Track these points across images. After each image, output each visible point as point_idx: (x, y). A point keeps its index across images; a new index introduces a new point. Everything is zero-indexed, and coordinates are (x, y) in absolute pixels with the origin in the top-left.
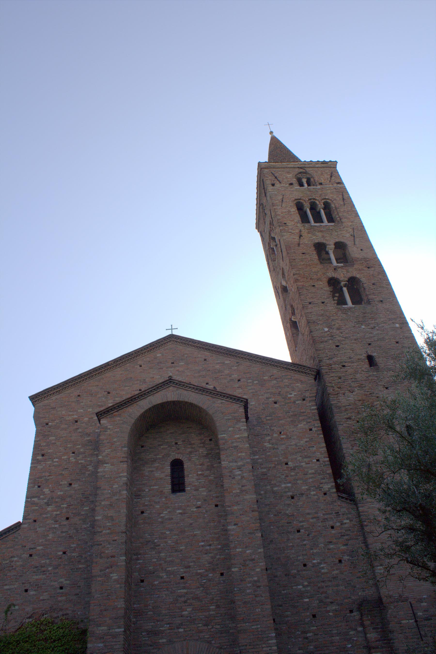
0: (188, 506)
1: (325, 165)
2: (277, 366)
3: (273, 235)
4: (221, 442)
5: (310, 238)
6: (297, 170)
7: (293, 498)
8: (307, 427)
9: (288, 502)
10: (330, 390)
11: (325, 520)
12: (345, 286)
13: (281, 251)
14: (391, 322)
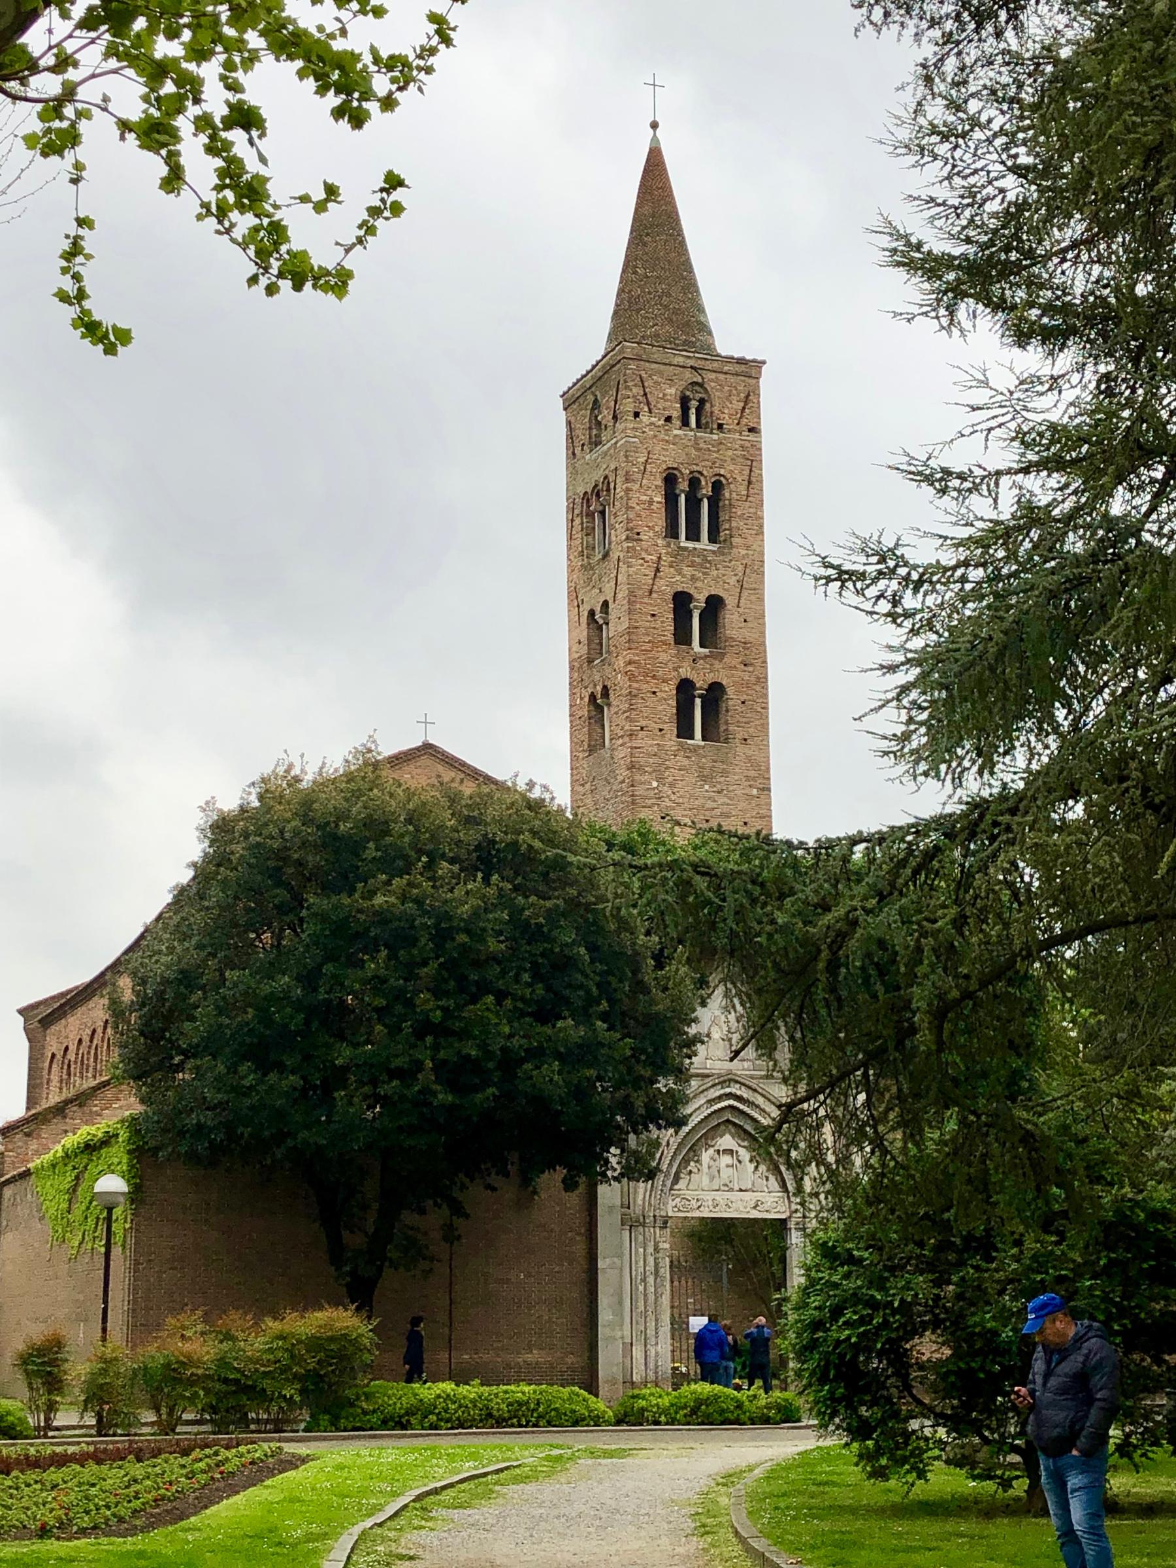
1: (743, 368)
5: (672, 581)
6: (690, 376)
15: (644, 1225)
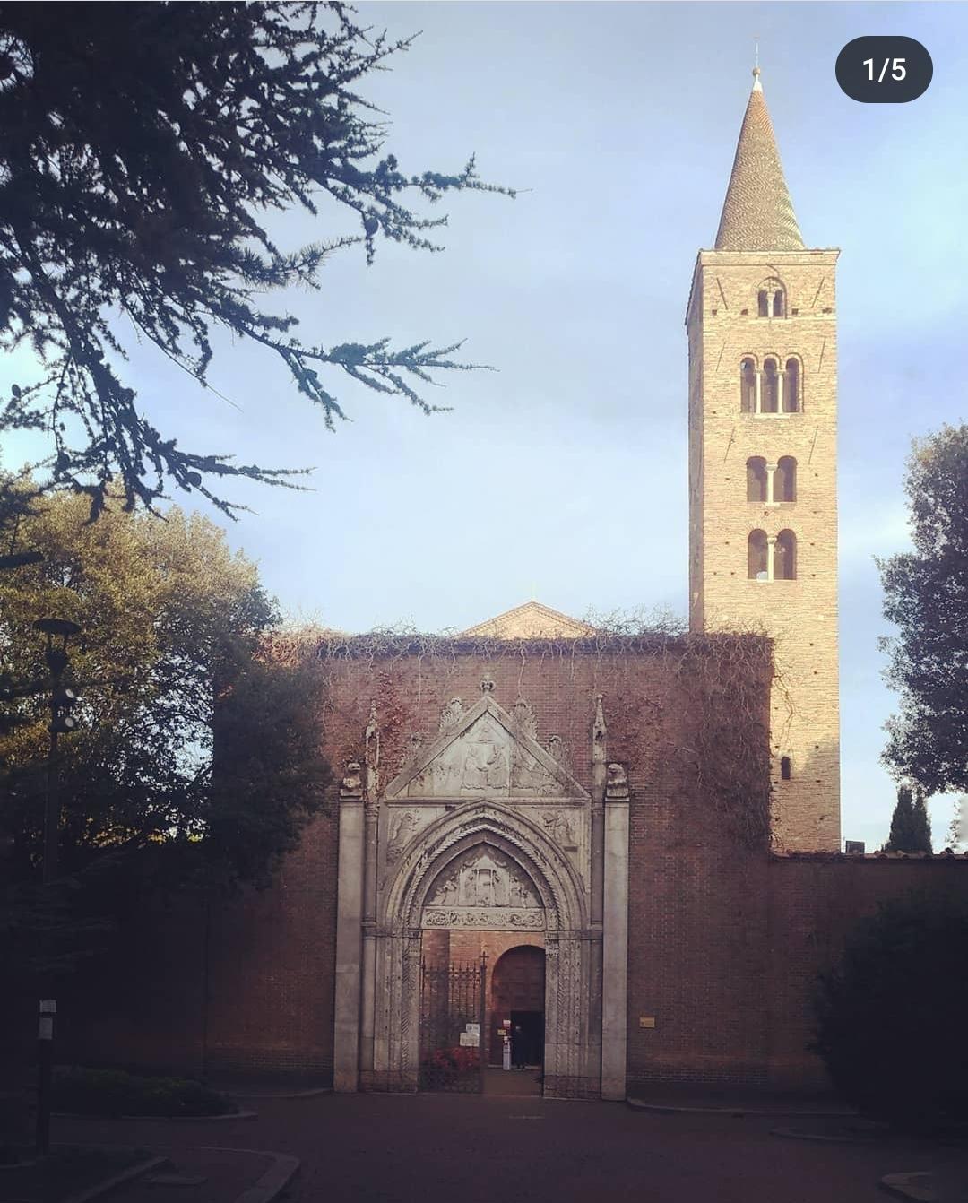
15: (390, 935)
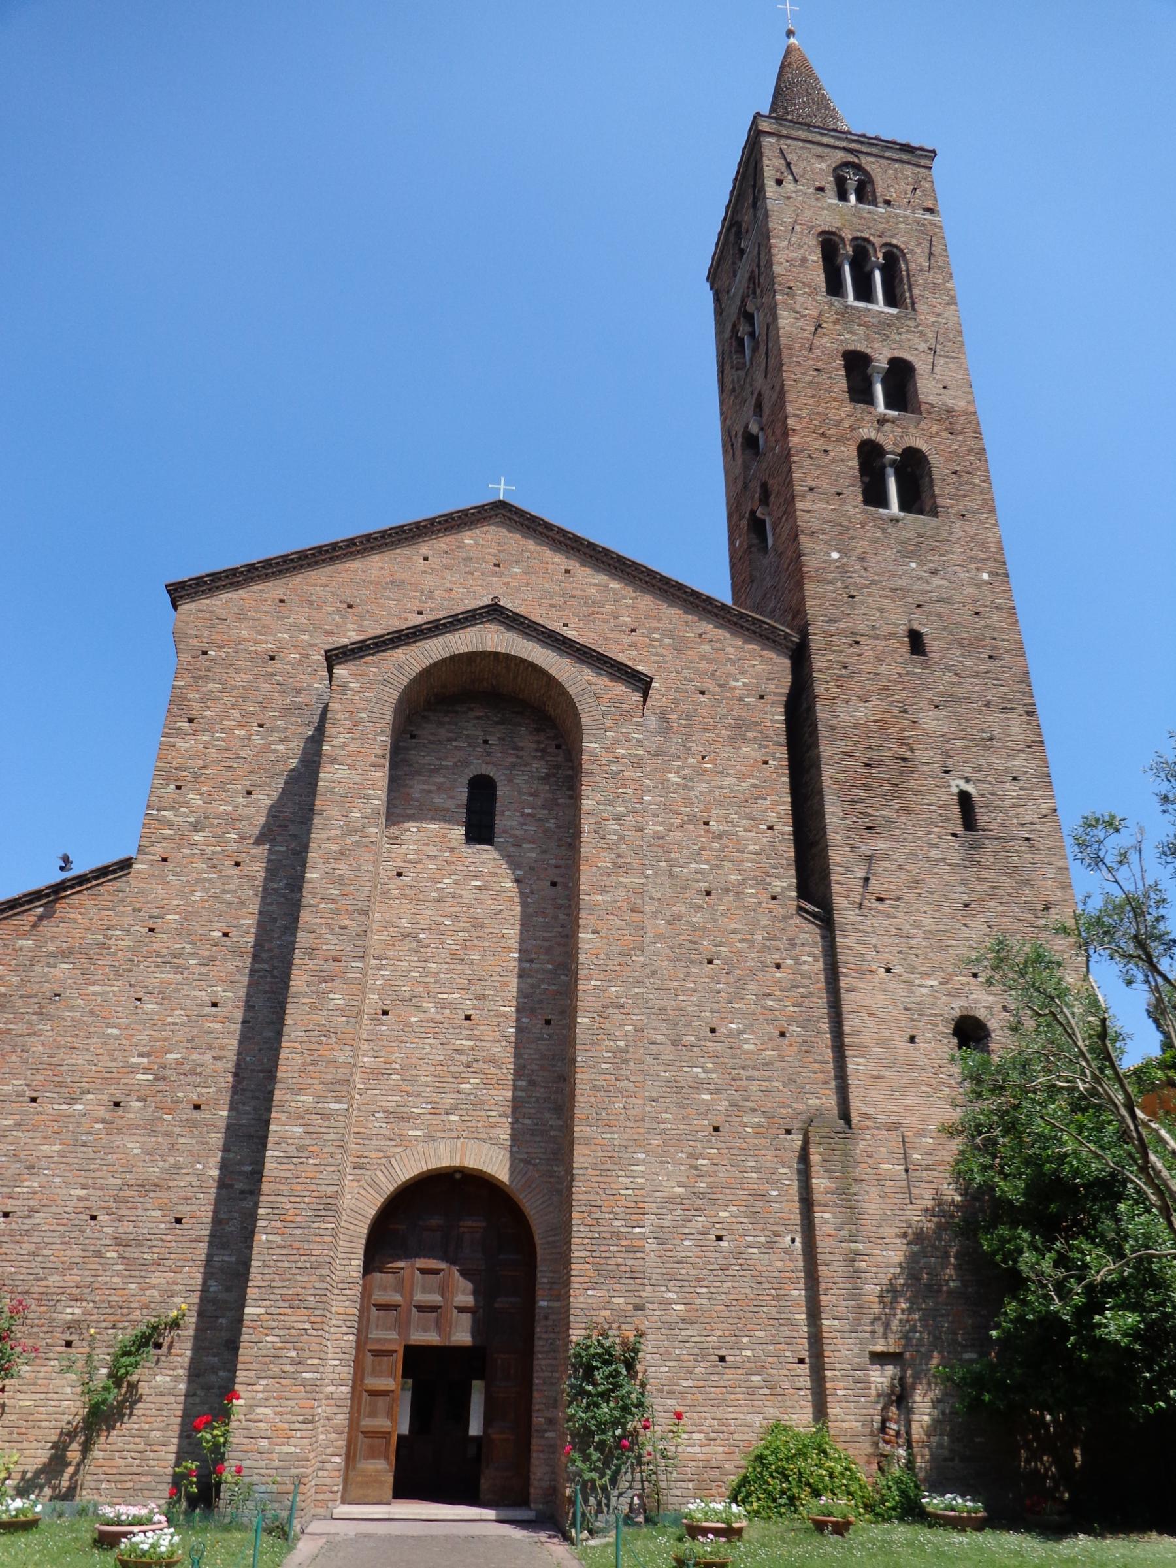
0: (496, 875)
2: (716, 615)
3: (750, 308)
4: (586, 757)
6: (841, 156)
7: (708, 894)
8: (759, 756)
9: (698, 900)
10: (819, 689)
11: (765, 949)
12: (891, 466)
13: (767, 353)
14: (973, 566)
